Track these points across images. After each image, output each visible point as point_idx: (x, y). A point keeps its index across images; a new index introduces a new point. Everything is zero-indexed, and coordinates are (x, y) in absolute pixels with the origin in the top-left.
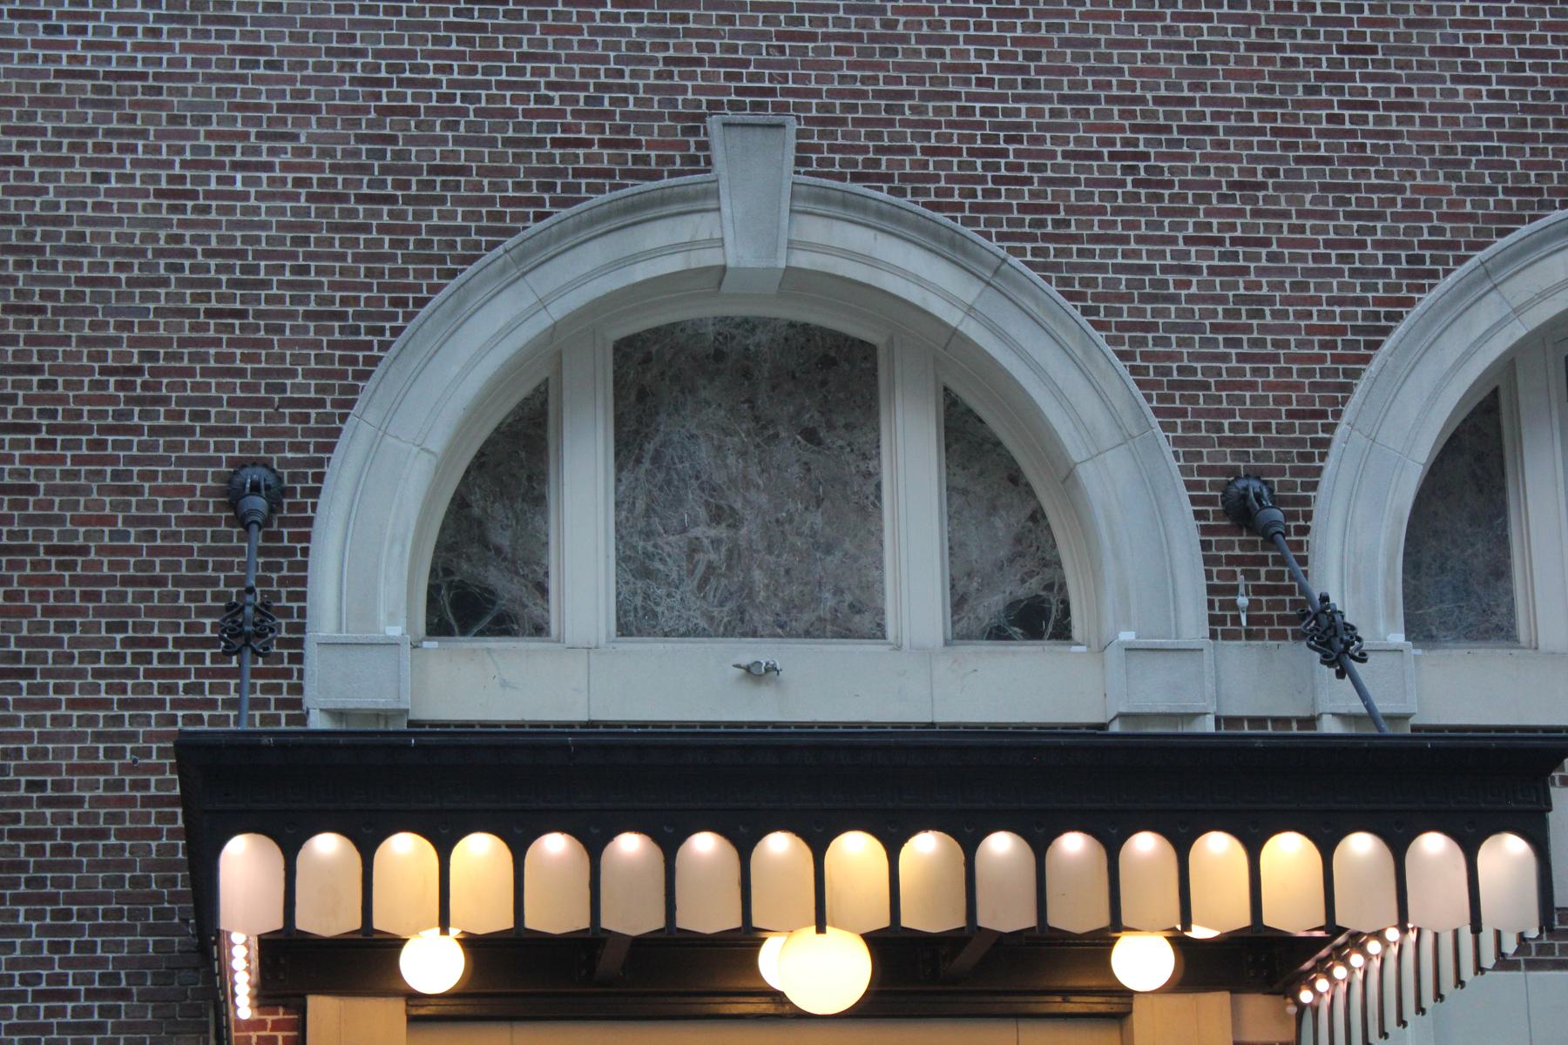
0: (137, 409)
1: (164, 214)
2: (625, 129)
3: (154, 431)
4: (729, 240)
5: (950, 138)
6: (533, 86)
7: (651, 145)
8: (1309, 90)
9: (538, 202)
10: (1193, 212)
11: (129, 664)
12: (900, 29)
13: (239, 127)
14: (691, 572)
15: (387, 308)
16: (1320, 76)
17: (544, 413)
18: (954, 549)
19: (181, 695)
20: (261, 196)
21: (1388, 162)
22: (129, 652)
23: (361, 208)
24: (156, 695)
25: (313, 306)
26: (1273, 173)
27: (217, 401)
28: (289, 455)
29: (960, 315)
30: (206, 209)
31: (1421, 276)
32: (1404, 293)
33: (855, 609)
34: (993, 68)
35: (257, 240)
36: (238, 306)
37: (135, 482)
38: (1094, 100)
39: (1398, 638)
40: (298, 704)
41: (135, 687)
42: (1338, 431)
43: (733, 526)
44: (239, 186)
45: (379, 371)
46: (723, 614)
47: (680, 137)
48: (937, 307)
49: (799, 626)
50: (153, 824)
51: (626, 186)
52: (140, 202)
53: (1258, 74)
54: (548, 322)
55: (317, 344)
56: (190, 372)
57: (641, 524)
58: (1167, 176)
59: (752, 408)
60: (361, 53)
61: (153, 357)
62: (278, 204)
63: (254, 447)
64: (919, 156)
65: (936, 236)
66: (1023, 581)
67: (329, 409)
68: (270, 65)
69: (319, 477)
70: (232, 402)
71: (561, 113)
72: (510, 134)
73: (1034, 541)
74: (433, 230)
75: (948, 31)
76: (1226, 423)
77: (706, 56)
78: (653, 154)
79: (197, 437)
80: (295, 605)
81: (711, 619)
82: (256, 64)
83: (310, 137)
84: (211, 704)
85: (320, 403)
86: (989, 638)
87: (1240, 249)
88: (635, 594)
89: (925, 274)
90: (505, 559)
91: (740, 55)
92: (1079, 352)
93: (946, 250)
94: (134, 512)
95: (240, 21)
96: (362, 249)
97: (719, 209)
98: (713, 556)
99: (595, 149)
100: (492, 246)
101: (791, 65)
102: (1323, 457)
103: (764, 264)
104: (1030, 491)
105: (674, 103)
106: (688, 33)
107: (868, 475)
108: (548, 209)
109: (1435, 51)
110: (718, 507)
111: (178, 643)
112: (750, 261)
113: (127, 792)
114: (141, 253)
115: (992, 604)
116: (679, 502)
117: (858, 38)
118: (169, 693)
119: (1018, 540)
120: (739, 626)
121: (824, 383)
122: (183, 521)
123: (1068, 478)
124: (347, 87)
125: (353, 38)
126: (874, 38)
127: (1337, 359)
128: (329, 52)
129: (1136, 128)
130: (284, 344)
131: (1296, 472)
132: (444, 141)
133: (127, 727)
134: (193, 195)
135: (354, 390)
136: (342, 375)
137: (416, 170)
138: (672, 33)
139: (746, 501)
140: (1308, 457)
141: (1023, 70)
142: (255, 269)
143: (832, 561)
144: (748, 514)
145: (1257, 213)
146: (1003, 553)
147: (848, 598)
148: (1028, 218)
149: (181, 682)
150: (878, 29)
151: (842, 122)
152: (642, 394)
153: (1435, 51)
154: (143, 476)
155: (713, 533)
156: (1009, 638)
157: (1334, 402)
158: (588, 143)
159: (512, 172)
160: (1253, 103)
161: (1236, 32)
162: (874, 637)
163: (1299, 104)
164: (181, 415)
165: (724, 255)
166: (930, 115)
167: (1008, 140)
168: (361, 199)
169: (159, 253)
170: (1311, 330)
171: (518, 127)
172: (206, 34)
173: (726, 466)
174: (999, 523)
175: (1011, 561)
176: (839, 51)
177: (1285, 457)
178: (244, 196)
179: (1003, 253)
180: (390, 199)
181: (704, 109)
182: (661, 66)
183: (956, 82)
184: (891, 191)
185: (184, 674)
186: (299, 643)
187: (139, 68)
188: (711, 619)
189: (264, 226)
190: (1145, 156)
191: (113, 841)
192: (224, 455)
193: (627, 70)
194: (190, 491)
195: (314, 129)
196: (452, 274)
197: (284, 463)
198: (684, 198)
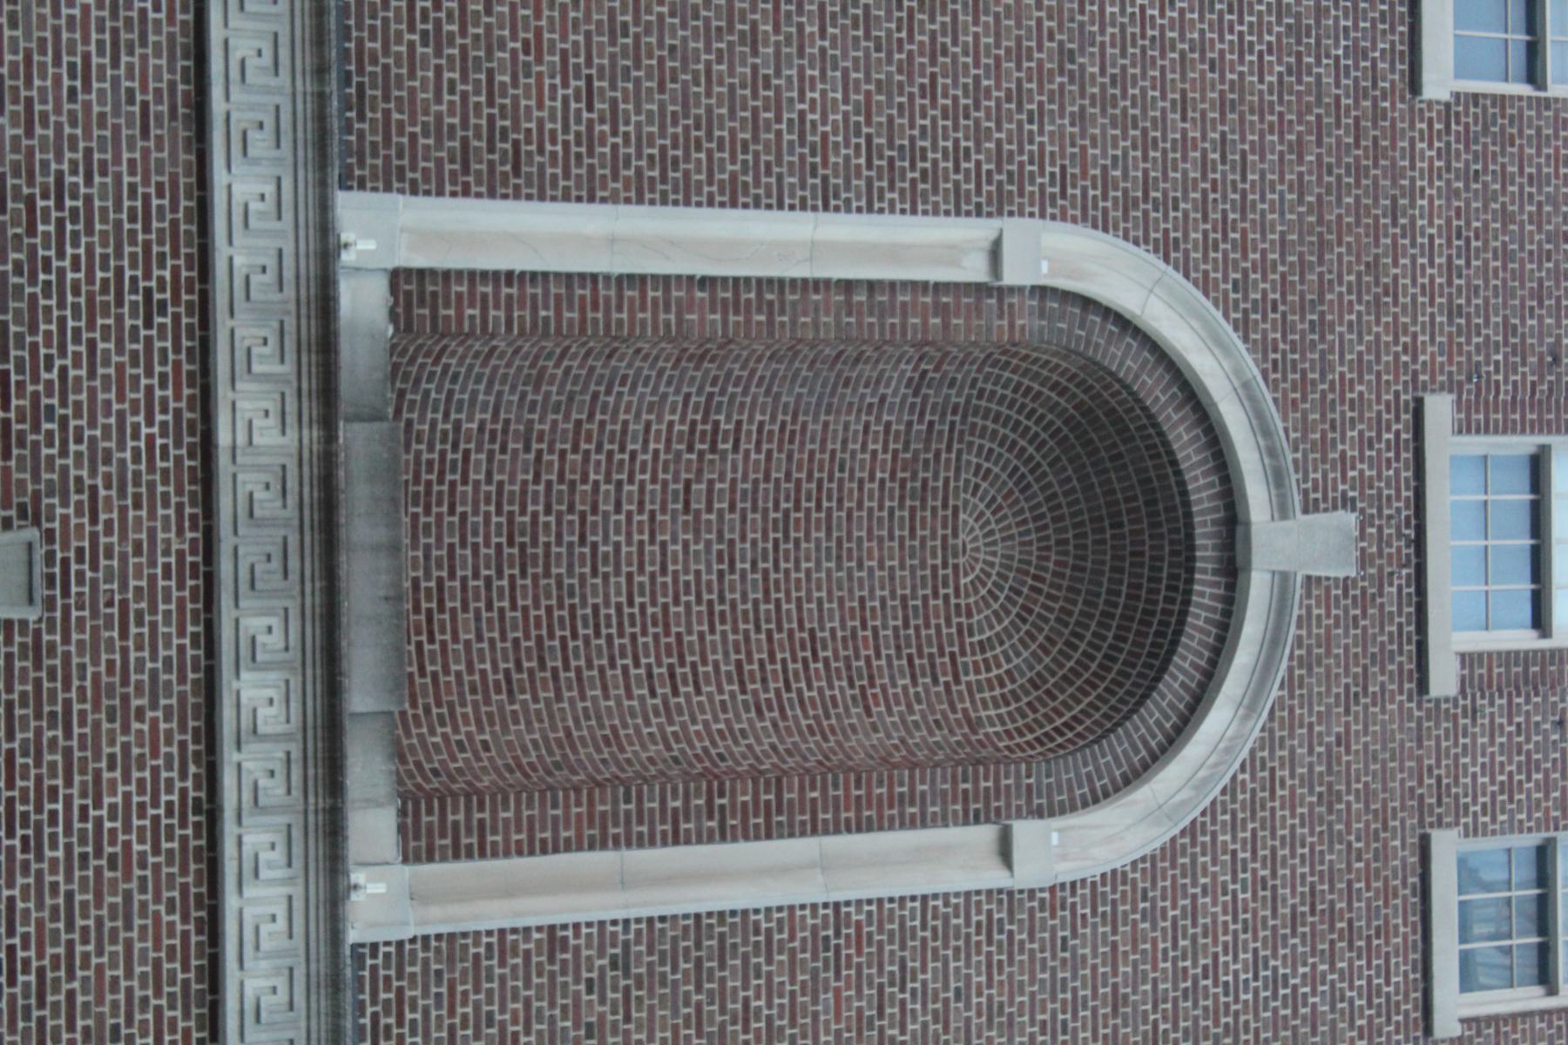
5: (25, 777)
6: (63, 352)
12: (135, 725)
34: (99, 822)
38: (70, 926)
60: (89, 181)
68: (72, 92)
71: (35, 379)
82: (72, 76)
95: (115, 63)
101: (95, 614)
105: (50, 494)
106: (123, 510)
117: (125, 682)
125: (104, 173)
126: (125, 699)
129: (41, 972)
138: (122, 493)
141: (98, 853)
151: (38, 666)
167: (25, 839)
176: (111, 664)
181: (45, 525)
182: (87, 482)
183: (84, 784)
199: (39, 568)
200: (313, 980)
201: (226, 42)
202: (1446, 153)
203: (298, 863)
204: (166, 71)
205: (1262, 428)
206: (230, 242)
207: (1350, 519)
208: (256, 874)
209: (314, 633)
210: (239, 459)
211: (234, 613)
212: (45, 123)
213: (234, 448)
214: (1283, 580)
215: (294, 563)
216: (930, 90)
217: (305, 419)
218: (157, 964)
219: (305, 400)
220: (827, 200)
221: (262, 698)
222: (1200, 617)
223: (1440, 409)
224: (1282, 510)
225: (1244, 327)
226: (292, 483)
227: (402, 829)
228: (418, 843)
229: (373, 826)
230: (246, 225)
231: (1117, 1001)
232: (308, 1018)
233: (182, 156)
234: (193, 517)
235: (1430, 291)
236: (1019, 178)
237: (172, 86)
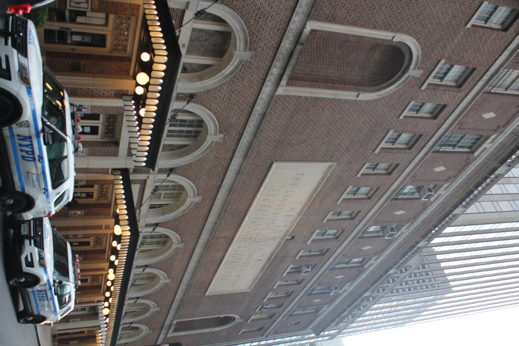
17: (224, 24)
31: (214, 114)
33: (190, 52)
39: (173, 108)
45: (234, 12)
73: (194, 70)
115: (187, 66)
120: (191, 40)
123: (200, 79)
202: (464, 34)
205: (418, 59)
207: (422, 72)
209: (284, 66)
214: (409, 76)
216: (396, 18)
220: (375, 28)
221: (275, 71)
222: (397, 76)
223: (443, 61)
224: (414, 69)
225: (422, 49)
228: (288, 84)
229: (284, 82)
231: (363, 110)
235: (451, 48)
236: (402, 29)
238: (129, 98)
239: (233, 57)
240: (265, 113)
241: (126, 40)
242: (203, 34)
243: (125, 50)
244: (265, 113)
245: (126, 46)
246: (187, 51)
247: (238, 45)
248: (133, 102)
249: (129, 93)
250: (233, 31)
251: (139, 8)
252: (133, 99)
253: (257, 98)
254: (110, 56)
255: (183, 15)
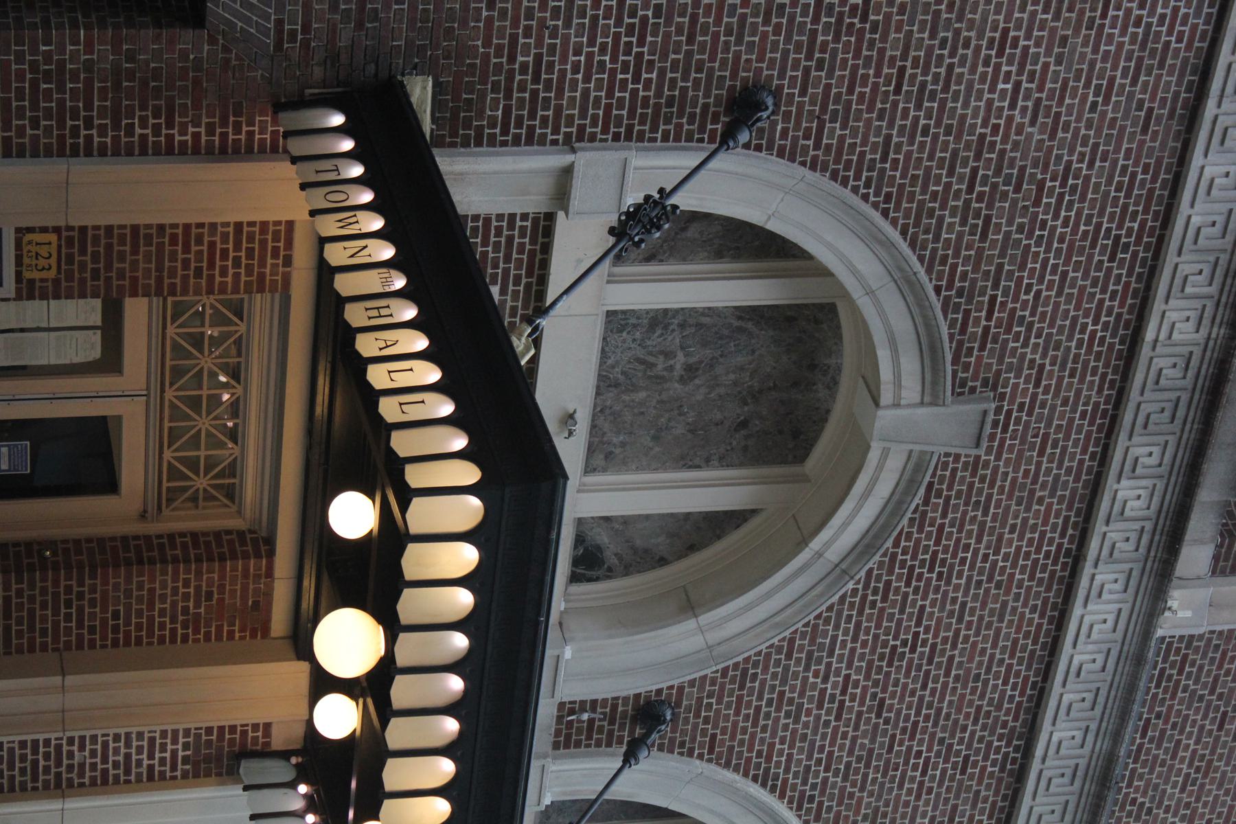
0: (833, 20)
1: (988, 34)
2: (995, 341)
3: (814, 33)
4: (898, 412)
7: (979, 358)
8: (941, 741)
9: (950, 287)
10: (867, 678)
11: (627, 20)
12: (1035, 507)
13: (1048, 85)
14: (650, 354)
15: (885, 189)
16: (950, 746)
18: (647, 517)
19: (597, 58)
20: (990, 102)
21: (882, 785)
22: (637, 21)
23: (968, 170)
24: (599, 40)
25: (895, 139)
26: (887, 722)
27: (830, 75)
28: (779, 128)
29: (817, 548)
30: (986, 63)
32: (788, 793)
33: (609, 456)
35: (955, 100)
36: (905, 88)
37: (774, 20)
38: (960, 620)
39: (547, 801)
40: (580, 139)
41: (608, 26)
42: (698, 762)
43: (682, 380)
44: (1001, 86)
45: (836, 187)
46: (616, 374)
47: (982, 375)
48: (825, 535)
49: (600, 422)
50: (495, 41)
51: (951, 342)
52: (1001, 18)
53: (959, 711)
54: (855, 296)
55: (864, 143)
56: (857, 55)
57: (692, 321)
58: (896, 663)
59: (770, 389)
60: (1091, 165)
61: (874, 29)
62: (982, 114)
63: (790, 101)
64: (939, 521)
65: (876, 537)
66: (616, 555)
67: (812, 153)
68: (1094, 104)
69: (758, 148)
70: (828, 86)
72: (1006, 267)
73: (643, 559)
74: (941, 219)
75: (1028, 535)
76: (714, 701)
77: (1041, 390)
78: (973, 359)
79: (803, 63)
80: (659, 135)
81: (613, 367)
82: (1096, 94)
83: (1031, 135)
84: (587, 79)
85: (817, 146)
86: (577, 535)
87: (836, 705)
88: (638, 318)
89: (851, 528)
90: (676, 234)
91: (1037, 410)
92: (777, 619)
93: (866, 541)
94: (750, 20)
96: (935, 171)
97: (922, 403)
98: (660, 367)
99: (984, 323)
100: (921, 259)
101: (1023, 442)
102: (681, 754)
103: (875, 433)
104: (681, 556)
105: (1009, 371)
106: (1060, 379)
107: (708, 461)
108: (943, 293)
109: (955, 807)
110: (697, 369)
111: (640, 55)
112: (878, 424)
113: (523, 23)
114: (960, 19)
115: (602, 537)
116: (705, 344)
117: (1034, 482)
118: (600, 50)
119: (646, 551)
120: (605, 383)
121: (781, 432)
122: (737, 56)
123: (690, 604)
124: (1066, 158)
126: (1032, 492)
127: (749, 760)
128: (1096, 145)
130: (869, 121)
131: (672, 740)
132: (1010, 223)
133: (575, 21)
134: (1000, 54)
135: (824, 169)
136: (837, 162)
137: (990, 206)
139: (699, 387)
140: (682, 744)
141: (990, 580)
142: (932, 97)
143: (647, 441)
144: (691, 387)
145: (860, 714)
146: (639, 543)
147: (618, 451)
148: (881, 585)
149: (607, 58)
150: (1038, 494)
151: (973, 475)
152: (791, 320)
153: (955, 807)
154: (778, 27)
155: (678, 366)
156: (576, 547)
157: (719, 758)
158: (989, 318)
159: (976, 269)
160: (939, 710)
161: (992, 699)
162: (587, 466)
163: (933, 735)
164: (823, 51)
165: (887, 407)
166: (967, 527)
167: (940, 574)
168: (975, 171)
169: (957, 32)
170: (772, 745)
171: (1011, 273)
172: (1129, 59)
173: (728, 373)
174: (660, 540)
175: (632, 548)
176: (1027, 472)
177: (684, 733)
178: (992, 90)
179: (857, 577)
180: (970, 189)
181: (1000, 390)
183: (989, 542)
184: (918, 505)
185: (614, 59)
186: (629, 138)
187: (1111, 13)
188: (613, 367)
189: (966, 105)
190: (913, 650)
191: (485, 13)
192: (786, 82)
193: (1041, 341)
194: (761, 59)
195: (1037, 137)
196: (904, 233)
197: (775, 123)
198: (934, 383)
199: (991, 417)
200: (1124, 655)
201: (1230, 65)
203: (1131, 590)
204: (1171, 83)
206: (1192, 206)
208: (1100, 595)
209: (1184, 457)
210: (1158, 349)
211: (1127, 444)
212: (1066, 130)
213: (1156, 341)
215: (1181, 413)
217: (1218, 320)
218: (1015, 641)
219: (1221, 309)
221: (1132, 496)
226: (1194, 362)
227: (1216, 558)
229: (1196, 555)
230: (1209, 193)
232: (1114, 675)
233: (1171, 144)
234: (1112, 382)
237: (1176, 95)
238: (284, 771)
239: (868, 447)
240: (1110, 759)
241: (233, 435)
242: (674, 340)
243: (231, 493)
244: (1110, 759)
245: (233, 469)
246: (591, 450)
247: (886, 373)
248: (303, 789)
249: (277, 743)
250: (846, 295)
251: (289, 244)
252: (303, 775)
253: (1047, 673)
254: (148, 538)
255: (547, 249)
